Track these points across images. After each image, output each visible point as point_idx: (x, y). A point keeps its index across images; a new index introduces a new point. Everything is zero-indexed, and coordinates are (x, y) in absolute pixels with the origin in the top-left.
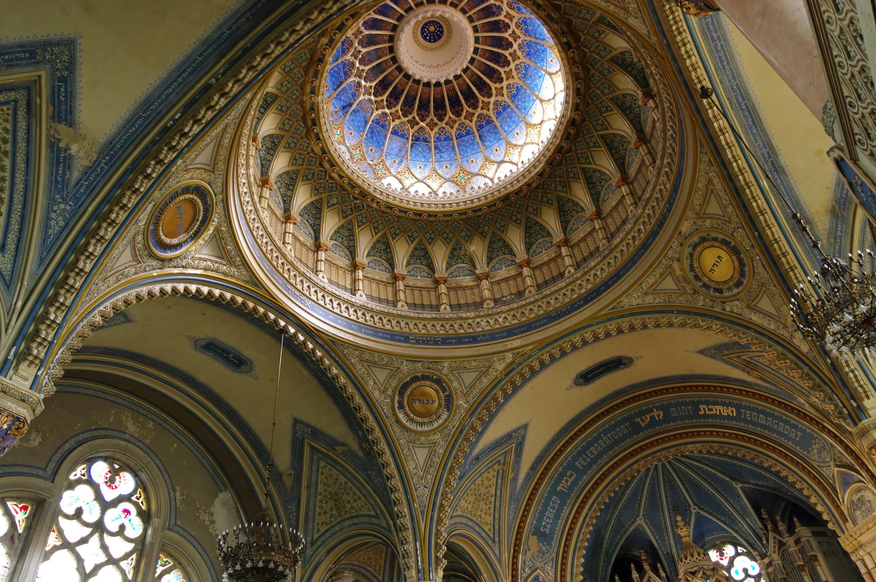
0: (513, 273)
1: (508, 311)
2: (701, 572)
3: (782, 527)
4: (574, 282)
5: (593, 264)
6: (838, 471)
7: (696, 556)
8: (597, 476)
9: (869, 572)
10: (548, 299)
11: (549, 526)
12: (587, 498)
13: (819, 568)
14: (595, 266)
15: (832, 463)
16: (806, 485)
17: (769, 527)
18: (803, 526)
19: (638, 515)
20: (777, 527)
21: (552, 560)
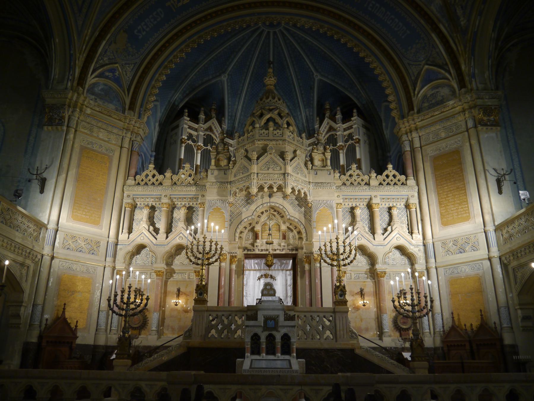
2: (278, 111)
3: (339, 116)
6: (427, 69)
7: (276, 99)
8: (210, 11)
9: (413, 150)
11: (144, 33)
12: (191, 26)
13: (357, 149)
15: (424, 62)
16: (388, 78)
17: (327, 115)
18: (358, 116)
19: (224, 72)
20: (335, 114)
21: (135, 64)
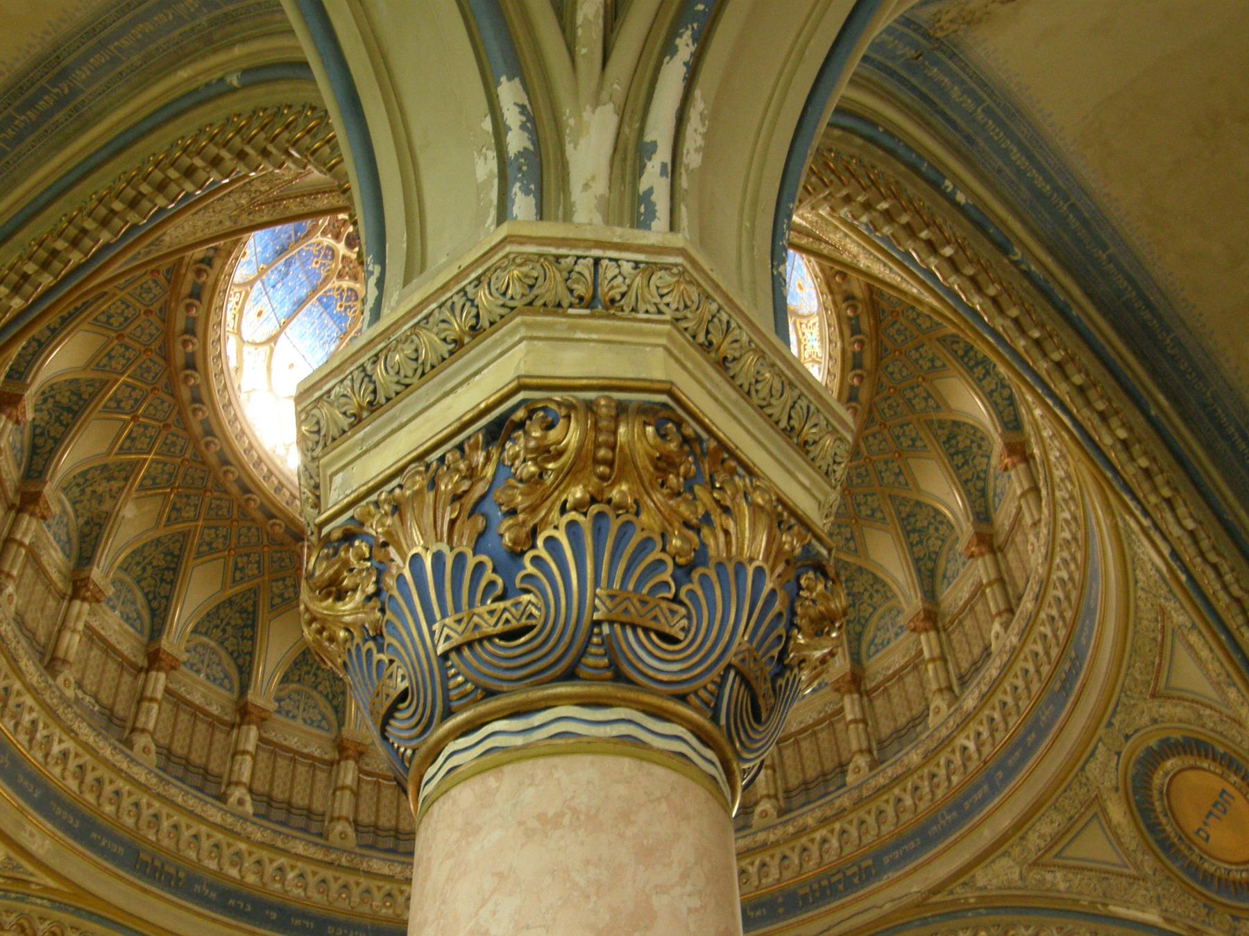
0: (125, 647)
1: (86, 746)
4: (237, 835)
5: (300, 848)
10: (165, 810)
14: (298, 856)
